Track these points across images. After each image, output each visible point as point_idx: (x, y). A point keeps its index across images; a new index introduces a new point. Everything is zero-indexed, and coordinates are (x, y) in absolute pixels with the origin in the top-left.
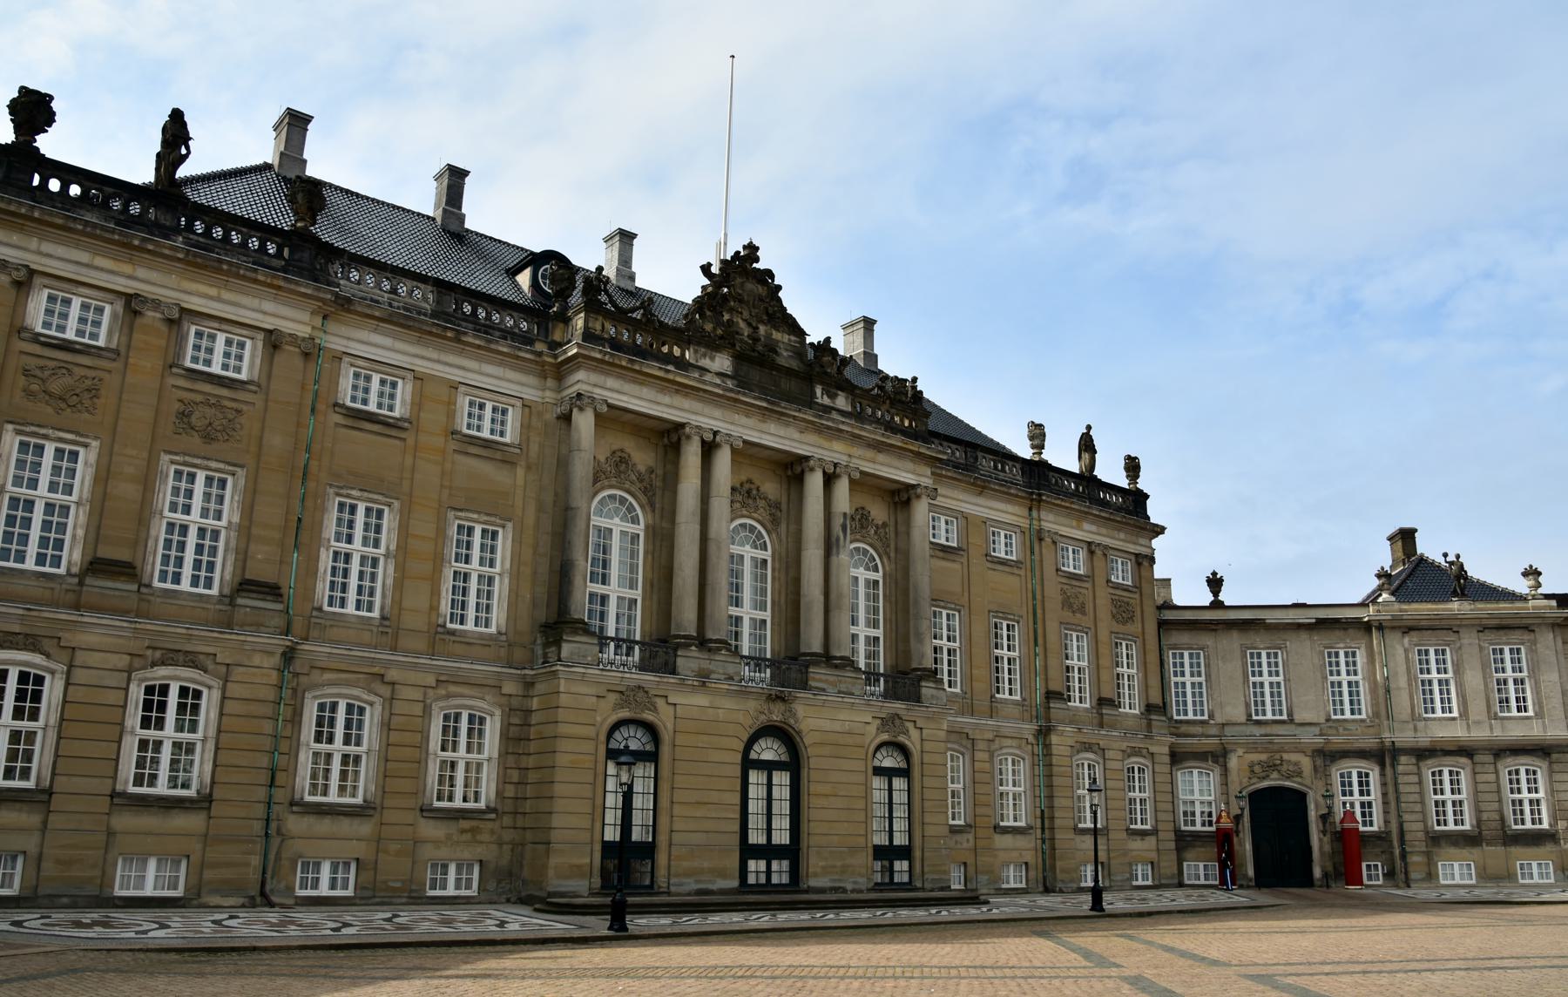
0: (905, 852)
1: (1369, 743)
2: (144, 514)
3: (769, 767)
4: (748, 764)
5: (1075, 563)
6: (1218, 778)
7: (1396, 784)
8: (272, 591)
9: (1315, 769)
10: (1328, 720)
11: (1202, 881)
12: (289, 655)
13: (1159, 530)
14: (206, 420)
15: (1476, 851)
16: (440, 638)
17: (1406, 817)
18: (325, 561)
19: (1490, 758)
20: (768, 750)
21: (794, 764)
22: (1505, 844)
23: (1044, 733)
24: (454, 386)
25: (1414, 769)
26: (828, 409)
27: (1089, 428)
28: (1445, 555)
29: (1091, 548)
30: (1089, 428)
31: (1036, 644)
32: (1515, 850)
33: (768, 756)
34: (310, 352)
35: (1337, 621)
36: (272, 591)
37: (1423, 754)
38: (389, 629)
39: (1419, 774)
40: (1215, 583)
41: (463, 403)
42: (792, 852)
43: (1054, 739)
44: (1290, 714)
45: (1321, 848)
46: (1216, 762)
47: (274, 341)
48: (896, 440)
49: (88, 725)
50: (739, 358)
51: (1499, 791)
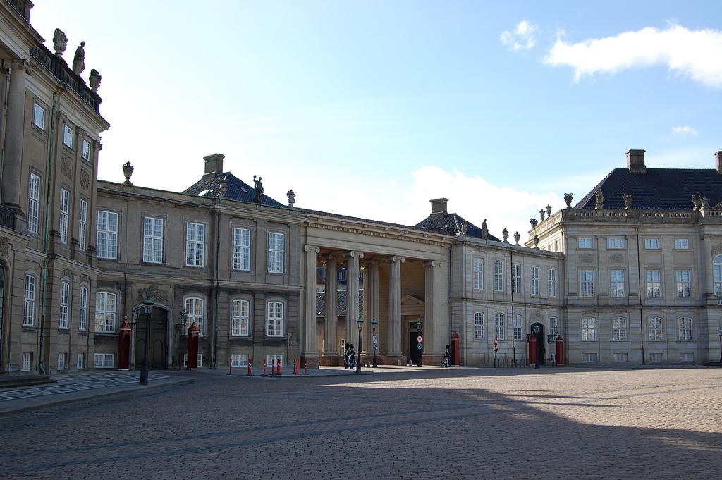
1: (205, 283)
6: (119, 299)
7: (216, 308)
9: (175, 296)
10: (184, 267)
11: (103, 366)
13: (106, 125)
15: (250, 348)
17: (219, 328)
19: (262, 296)
22: (263, 345)
25: (226, 299)
27: (83, 44)
28: (255, 177)
30: (83, 44)
31: (48, 196)
32: (269, 349)
35: (197, 206)
37: (232, 292)
39: (228, 303)
40: (128, 169)
44: (164, 261)
45: (173, 346)
46: (119, 288)
51: (264, 315)
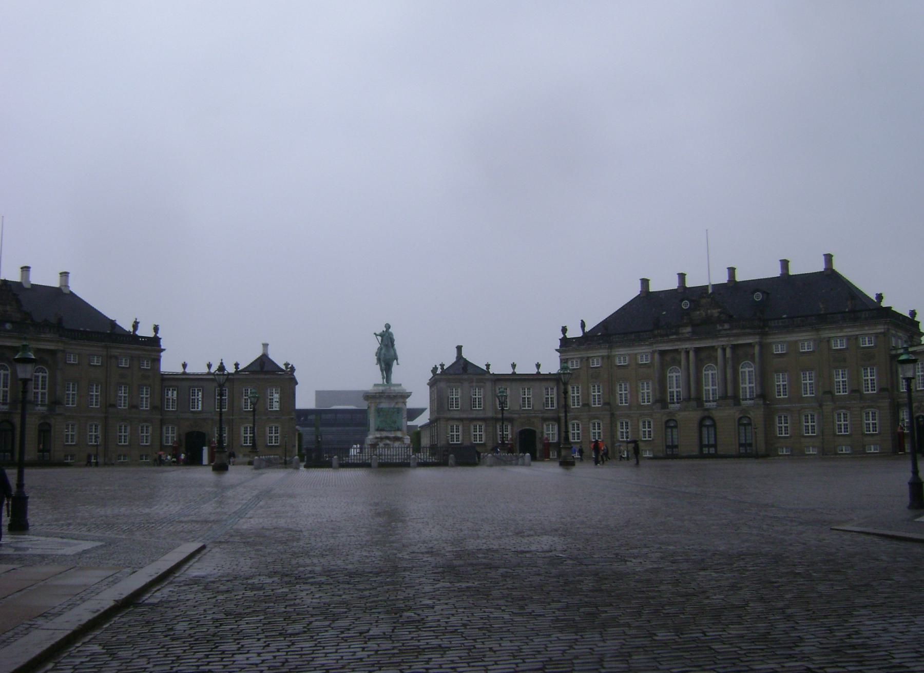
0: (750, 445)
2: (588, 395)
3: (708, 426)
4: (701, 425)
5: (838, 345)
8: (608, 404)
12: (612, 415)
14: (595, 375)
16: (640, 407)
18: (618, 396)
20: (708, 423)
21: (714, 425)
23: (821, 406)
24: (636, 354)
26: (720, 330)
29: (849, 338)
33: (708, 423)
34: (608, 357)
36: (608, 404)
38: (630, 407)
41: (639, 357)
42: (715, 446)
43: (824, 407)
47: (603, 357)
48: (747, 331)
49: (586, 431)
50: (694, 326)
